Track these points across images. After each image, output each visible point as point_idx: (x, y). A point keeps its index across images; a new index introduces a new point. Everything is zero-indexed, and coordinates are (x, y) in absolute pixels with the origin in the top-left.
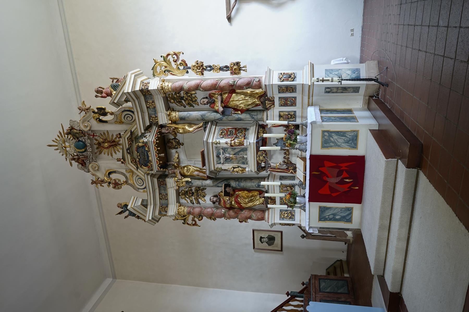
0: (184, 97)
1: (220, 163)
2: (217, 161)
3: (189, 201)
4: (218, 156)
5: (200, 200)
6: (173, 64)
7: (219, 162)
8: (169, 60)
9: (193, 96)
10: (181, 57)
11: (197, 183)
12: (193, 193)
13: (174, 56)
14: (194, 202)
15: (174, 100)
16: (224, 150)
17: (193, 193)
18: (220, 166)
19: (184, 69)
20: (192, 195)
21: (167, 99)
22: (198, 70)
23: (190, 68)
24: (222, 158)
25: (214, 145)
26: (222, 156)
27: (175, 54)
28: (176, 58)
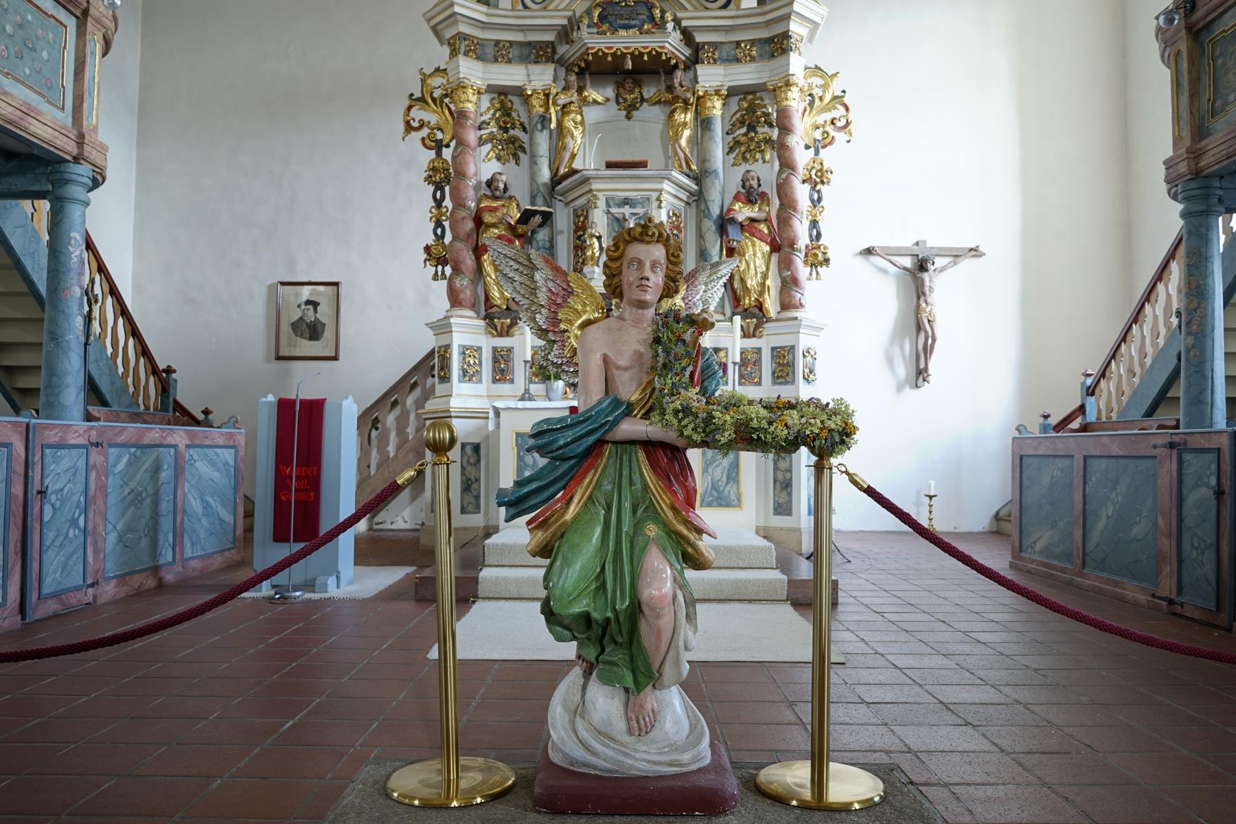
0: (756, 133)
1: (608, 205)
2: (613, 198)
3: (486, 118)
4: (626, 202)
5: (489, 146)
6: (828, 116)
7: (611, 203)
8: (835, 108)
9: (758, 156)
10: (840, 137)
11: (543, 142)
12: (506, 130)
14: (483, 132)
15: (746, 109)
17: (506, 130)
18: (601, 204)
20: (500, 128)
21: (749, 93)
22: (814, 171)
23: (817, 153)
24: (621, 210)
25: (655, 195)
26: (627, 210)
27: (848, 124)
28: (839, 124)
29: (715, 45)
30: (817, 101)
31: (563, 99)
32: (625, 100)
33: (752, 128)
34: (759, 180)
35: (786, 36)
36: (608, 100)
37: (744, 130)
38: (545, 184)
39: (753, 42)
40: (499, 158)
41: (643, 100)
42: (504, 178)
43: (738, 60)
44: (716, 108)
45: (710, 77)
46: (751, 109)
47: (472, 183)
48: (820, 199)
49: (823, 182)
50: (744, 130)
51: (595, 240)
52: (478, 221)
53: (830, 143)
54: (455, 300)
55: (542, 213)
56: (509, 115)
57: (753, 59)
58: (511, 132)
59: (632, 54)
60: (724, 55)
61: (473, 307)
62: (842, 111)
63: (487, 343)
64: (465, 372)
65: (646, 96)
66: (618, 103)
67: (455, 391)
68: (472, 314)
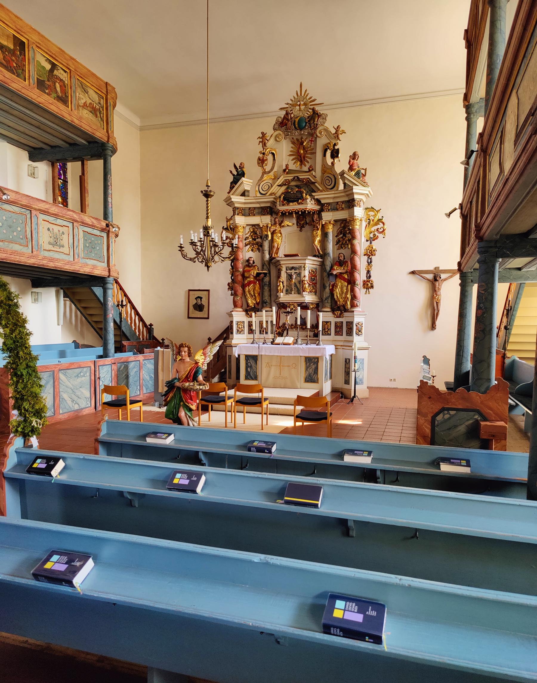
0: (346, 237)
1: (287, 270)
4: (292, 268)
6: (376, 228)
12: (255, 240)
13: (382, 229)
16: (299, 274)
17: (255, 240)
18: (284, 269)
19: (370, 238)
23: (371, 243)
25: (303, 265)
26: (293, 271)
28: (380, 230)
29: (329, 204)
30: (371, 222)
31: (273, 228)
32: (300, 224)
33: (344, 235)
34: (344, 256)
35: (353, 200)
36: (294, 224)
37: (342, 235)
38: (267, 261)
39: (343, 202)
40: (252, 250)
41: (307, 223)
42: (252, 259)
43: (337, 210)
44: (330, 230)
45: (327, 216)
46: (344, 227)
47: (240, 262)
48: (371, 262)
49: (372, 255)
50: (342, 235)
51: (281, 283)
52: (243, 276)
53: (376, 239)
54: (235, 306)
55: (263, 273)
56: (256, 234)
57: (343, 209)
58: (257, 240)
59: (295, 212)
60: (333, 207)
61: (242, 307)
62: (381, 225)
63: (246, 320)
64: (238, 330)
65: (308, 222)
66: (297, 225)
67: (234, 337)
68: (241, 310)
